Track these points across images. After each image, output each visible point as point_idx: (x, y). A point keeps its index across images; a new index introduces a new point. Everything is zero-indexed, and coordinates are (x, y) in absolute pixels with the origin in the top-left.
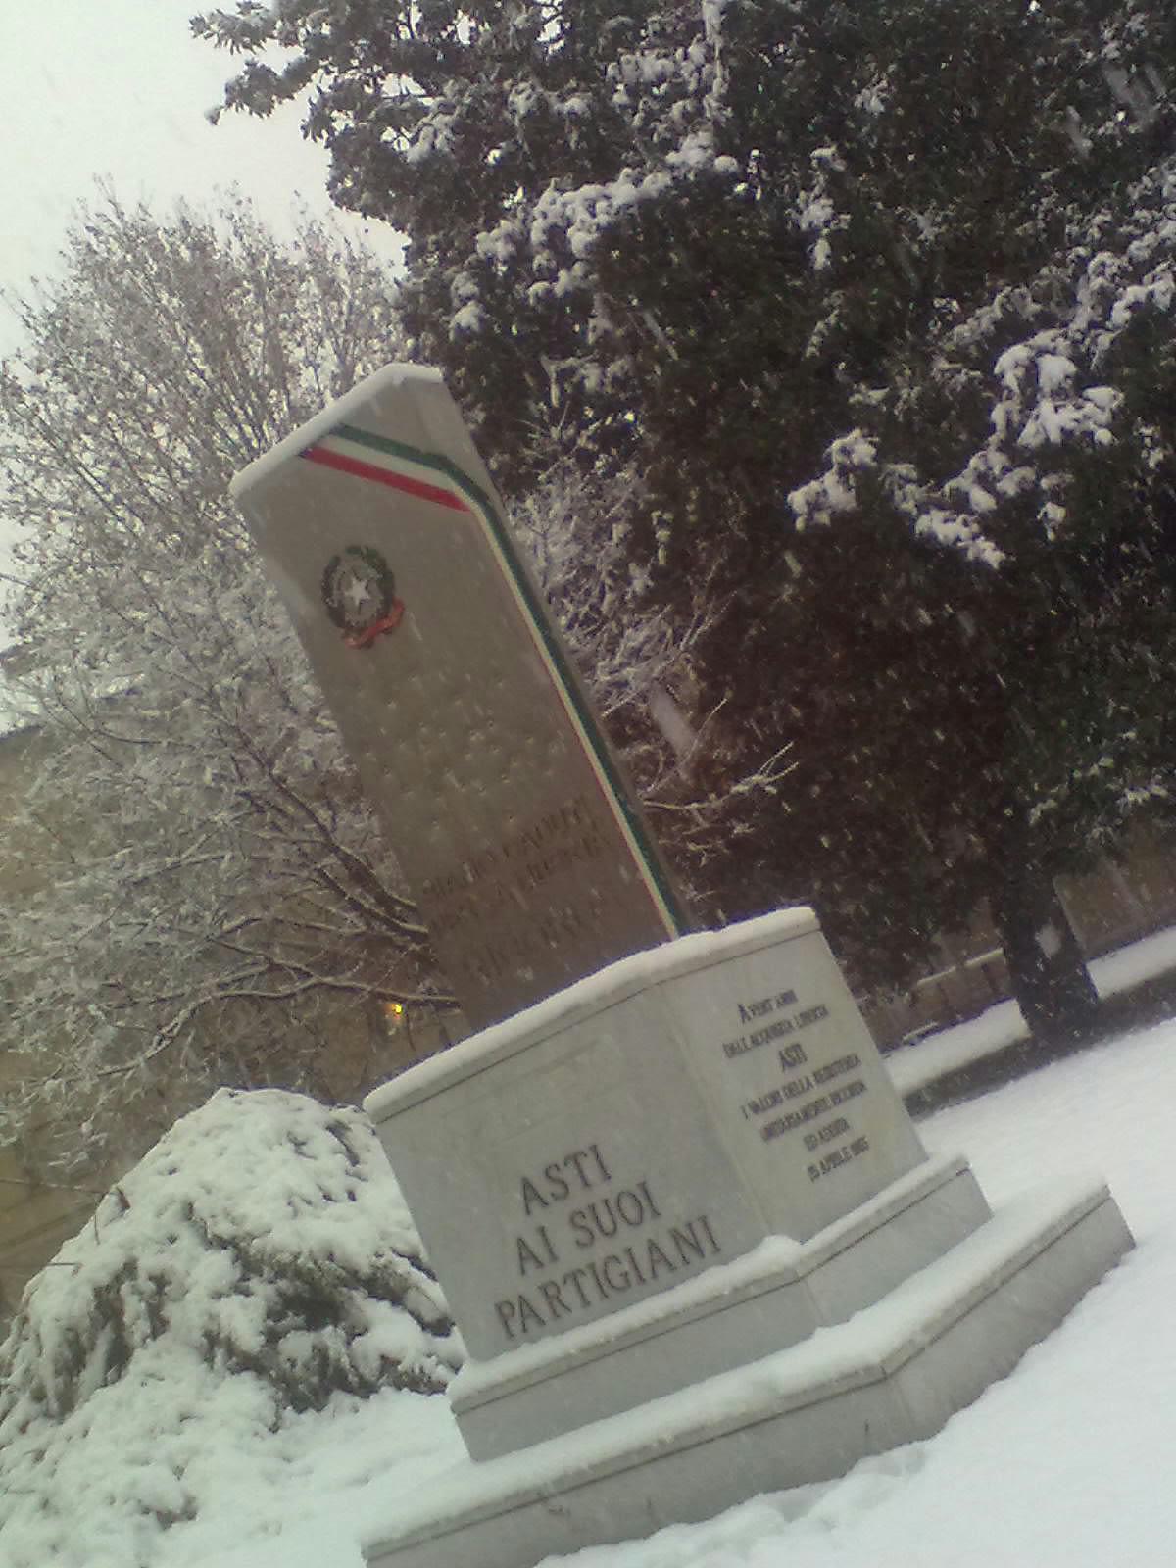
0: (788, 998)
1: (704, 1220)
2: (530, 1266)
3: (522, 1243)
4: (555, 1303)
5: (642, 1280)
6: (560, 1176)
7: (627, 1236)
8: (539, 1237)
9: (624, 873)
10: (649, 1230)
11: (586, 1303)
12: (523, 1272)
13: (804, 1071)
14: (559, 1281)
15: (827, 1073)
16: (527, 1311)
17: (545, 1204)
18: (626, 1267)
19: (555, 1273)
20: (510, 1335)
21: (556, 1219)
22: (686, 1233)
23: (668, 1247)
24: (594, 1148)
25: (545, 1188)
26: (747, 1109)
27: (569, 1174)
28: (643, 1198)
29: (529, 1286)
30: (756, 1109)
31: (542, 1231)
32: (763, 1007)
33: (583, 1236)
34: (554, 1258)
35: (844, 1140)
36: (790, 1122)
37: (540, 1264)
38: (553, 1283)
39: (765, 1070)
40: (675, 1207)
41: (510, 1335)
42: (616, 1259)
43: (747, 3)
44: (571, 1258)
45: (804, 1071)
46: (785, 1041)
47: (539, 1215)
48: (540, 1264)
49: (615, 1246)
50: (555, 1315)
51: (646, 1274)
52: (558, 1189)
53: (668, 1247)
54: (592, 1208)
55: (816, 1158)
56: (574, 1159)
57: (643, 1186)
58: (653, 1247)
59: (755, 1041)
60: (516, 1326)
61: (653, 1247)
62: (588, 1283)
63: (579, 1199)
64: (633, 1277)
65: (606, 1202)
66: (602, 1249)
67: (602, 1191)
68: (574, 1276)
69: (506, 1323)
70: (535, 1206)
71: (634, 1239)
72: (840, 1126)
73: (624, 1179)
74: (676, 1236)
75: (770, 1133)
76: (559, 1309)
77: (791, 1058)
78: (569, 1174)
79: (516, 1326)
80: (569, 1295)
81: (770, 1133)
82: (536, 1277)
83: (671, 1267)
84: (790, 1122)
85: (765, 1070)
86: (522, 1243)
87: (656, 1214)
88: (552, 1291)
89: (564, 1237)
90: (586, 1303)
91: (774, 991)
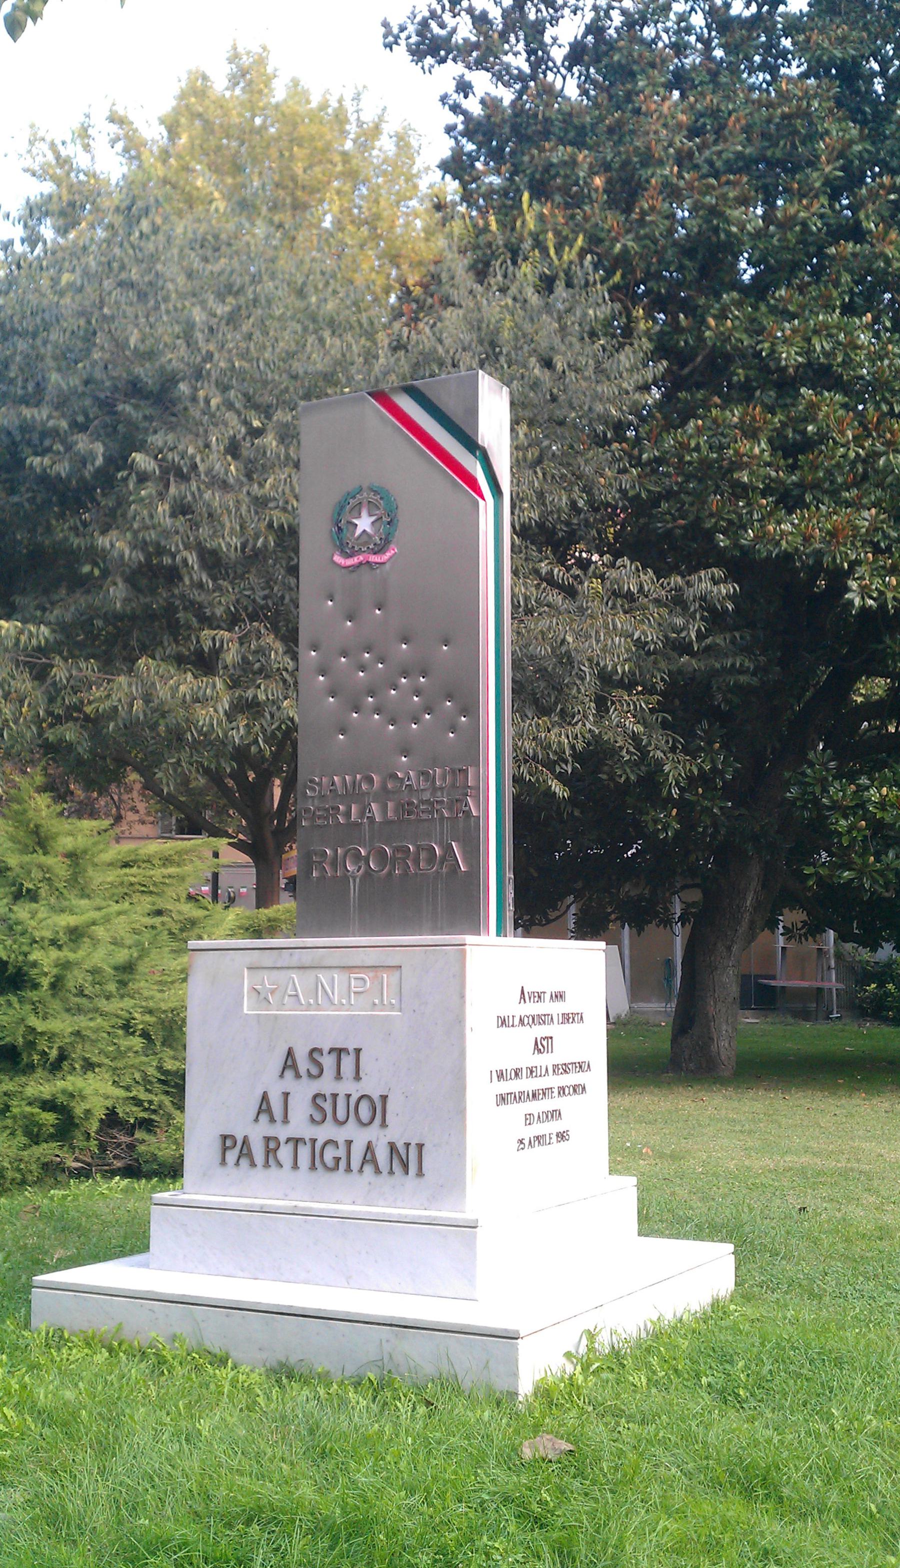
0: (559, 996)
1: (420, 1146)
2: (264, 1118)
3: (265, 1097)
4: (271, 1155)
5: (349, 1169)
6: (321, 1060)
7: (351, 1131)
8: (282, 1099)
9: (59, 1253)
10: (373, 1133)
11: (295, 1166)
12: (256, 1120)
13: (545, 1060)
14: (282, 1140)
15: (564, 1068)
16: (245, 1151)
17: (298, 1076)
18: (341, 1152)
19: (282, 1133)
20: (223, 1162)
21: (302, 1094)
22: (402, 1151)
23: (382, 1155)
24: (358, 1051)
25: (303, 1065)
26: (494, 1074)
27: (328, 1062)
28: (378, 1109)
29: (257, 1133)
30: (501, 1075)
31: (286, 1095)
32: (539, 996)
33: (318, 1117)
34: (286, 1120)
35: (553, 1127)
36: (519, 1097)
37: (272, 1120)
38: (276, 1139)
39: (517, 1047)
40: (399, 1129)
41: (223, 1162)
42: (335, 1143)
43: (738, 8)
44: (299, 1123)
45: (545, 1060)
46: (541, 1031)
47: (289, 1082)
48: (272, 1120)
49: (341, 1135)
50: (267, 1165)
51: (355, 1163)
52: (314, 1071)
53: (382, 1155)
54: (335, 1096)
55: (529, 1132)
56: (339, 1052)
57: (384, 1098)
58: (369, 1147)
59: (521, 1021)
60: (232, 1156)
61: (369, 1147)
62: (304, 1153)
63: (326, 1085)
64: (343, 1164)
65: (348, 1096)
66: (323, 1133)
67: (348, 1086)
68: (297, 1142)
69: (259, 1113)
70: (289, 1074)
71: (360, 1137)
72: (555, 1114)
73: (371, 1085)
74: (392, 1147)
75: (503, 1099)
76: (271, 1161)
77: (541, 1046)
78: (328, 1062)
79: (232, 1156)
80: (285, 1153)
81: (503, 1099)
82: (263, 1128)
83: (378, 1171)
84: (519, 1097)
85: (517, 1047)
86: (265, 1097)
87: (384, 1124)
88: (272, 1145)
89: (300, 1109)
90: (295, 1166)
91: (550, 988)
